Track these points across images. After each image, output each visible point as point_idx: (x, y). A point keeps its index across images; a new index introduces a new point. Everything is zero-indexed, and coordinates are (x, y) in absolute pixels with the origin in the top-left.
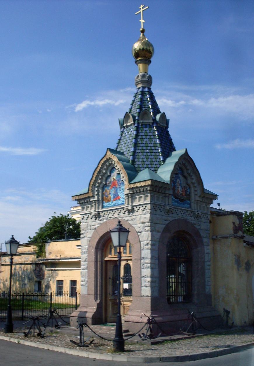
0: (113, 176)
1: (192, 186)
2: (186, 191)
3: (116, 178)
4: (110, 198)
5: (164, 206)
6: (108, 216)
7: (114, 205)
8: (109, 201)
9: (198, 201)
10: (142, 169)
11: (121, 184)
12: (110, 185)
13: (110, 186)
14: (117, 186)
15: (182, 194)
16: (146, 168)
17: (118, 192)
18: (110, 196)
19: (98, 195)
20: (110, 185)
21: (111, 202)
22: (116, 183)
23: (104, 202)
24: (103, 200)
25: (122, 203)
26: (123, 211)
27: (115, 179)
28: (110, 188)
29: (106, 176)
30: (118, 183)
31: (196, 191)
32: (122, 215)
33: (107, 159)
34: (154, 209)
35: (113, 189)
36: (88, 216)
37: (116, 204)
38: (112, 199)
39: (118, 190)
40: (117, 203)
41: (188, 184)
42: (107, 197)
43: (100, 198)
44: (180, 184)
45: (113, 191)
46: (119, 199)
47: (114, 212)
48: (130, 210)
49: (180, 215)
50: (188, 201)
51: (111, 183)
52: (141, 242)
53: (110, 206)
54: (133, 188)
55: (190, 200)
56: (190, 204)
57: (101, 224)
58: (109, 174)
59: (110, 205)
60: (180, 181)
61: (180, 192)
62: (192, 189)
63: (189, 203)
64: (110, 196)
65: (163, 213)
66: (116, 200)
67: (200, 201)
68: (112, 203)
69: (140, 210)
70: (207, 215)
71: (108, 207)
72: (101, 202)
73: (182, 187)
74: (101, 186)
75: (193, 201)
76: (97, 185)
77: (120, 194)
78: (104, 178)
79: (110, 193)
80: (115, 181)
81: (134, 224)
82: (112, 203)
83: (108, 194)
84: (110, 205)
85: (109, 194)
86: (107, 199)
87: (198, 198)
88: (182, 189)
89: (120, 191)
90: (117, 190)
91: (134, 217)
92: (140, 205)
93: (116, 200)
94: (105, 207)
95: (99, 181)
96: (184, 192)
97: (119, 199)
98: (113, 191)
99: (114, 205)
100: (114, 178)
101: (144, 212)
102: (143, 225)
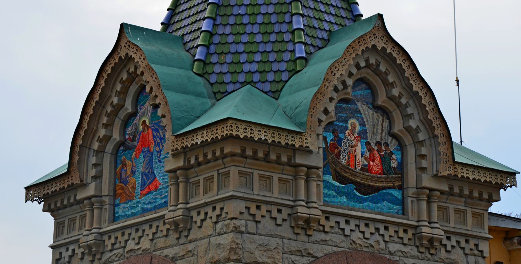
0: (144, 114)
1: (407, 140)
2: (385, 160)
3: (151, 121)
5: (292, 207)
6: (124, 247)
7: (144, 211)
9: (431, 190)
10: (230, 88)
12: (135, 143)
15: (366, 169)
16: (244, 83)
19: (97, 177)
21: (134, 201)
26: (164, 228)
27: (147, 123)
29: (122, 114)
31: (423, 156)
32: (160, 242)
34: (251, 218)
36: (73, 250)
38: (138, 190)
41: (394, 136)
44: (362, 135)
47: (140, 233)
49: (356, 236)
50: (397, 193)
54: (185, 149)
55: (401, 188)
56: (403, 203)
58: (129, 107)
59: (133, 211)
60: (362, 124)
61: (361, 161)
62: (411, 152)
63: (400, 197)
64: (132, 180)
65: (285, 230)
67: (442, 192)
69: (208, 223)
70: (472, 242)
73: (368, 144)
74: (110, 148)
75: (411, 192)
76: (96, 146)
78: (118, 123)
79: (133, 172)
82: (139, 202)
84: (133, 211)
85: (130, 176)
87: (427, 182)
88: (370, 150)
90: (151, 160)
92: (206, 204)
93: (148, 193)
95: (102, 132)
96: (377, 161)
100: (144, 122)
101: (219, 225)
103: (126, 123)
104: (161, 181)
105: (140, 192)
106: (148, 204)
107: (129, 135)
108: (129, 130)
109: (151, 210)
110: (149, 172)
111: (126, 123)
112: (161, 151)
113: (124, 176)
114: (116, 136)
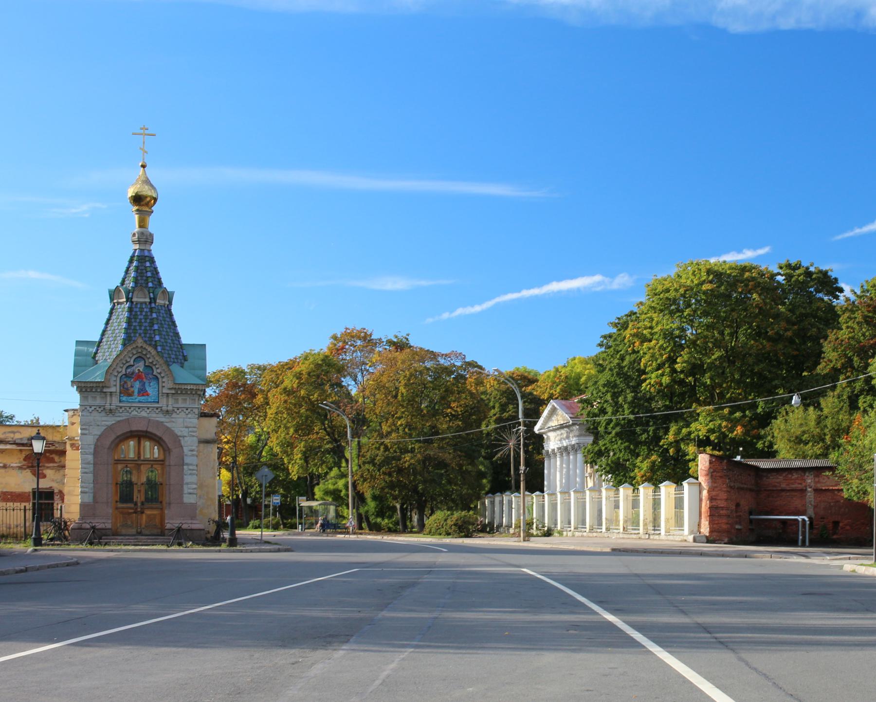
3: (144, 370)
4: (133, 392)
7: (140, 402)
18: (132, 389)
22: (144, 376)
24: (120, 393)
27: (141, 370)
29: (127, 364)
33: (137, 347)
35: (138, 382)
38: (136, 393)
39: (147, 385)
42: (127, 389)
43: (118, 391)
45: (137, 385)
46: (148, 395)
52: (184, 448)
53: (132, 402)
57: (119, 422)
58: (132, 363)
66: (143, 395)
71: (130, 402)
72: (118, 394)
74: (120, 375)
77: (149, 390)
79: (132, 387)
80: (140, 373)
81: (174, 427)
83: (129, 386)
91: (173, 420)
97: (148, 395)
98: (137, 385)
99: (140, 402)
100: (139, 370)
101: (189, 416)
102: (187, 429)
103: (127, 368)
108: (129, 370)
109: (144, 402)
111: (127, 368)
112: (150, 383)
113: (125, 386)
114: (124, 372)
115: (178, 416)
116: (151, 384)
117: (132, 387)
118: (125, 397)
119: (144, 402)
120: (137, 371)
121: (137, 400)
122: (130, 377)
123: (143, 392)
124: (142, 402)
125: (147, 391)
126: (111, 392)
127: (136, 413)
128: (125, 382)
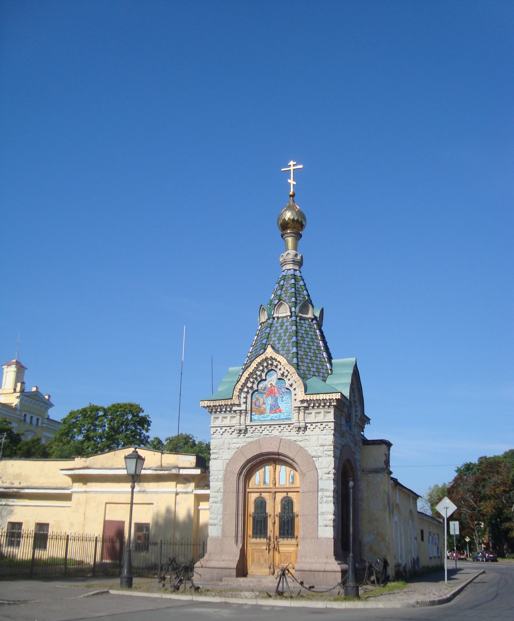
3: (277, 383)
4: (265, 409)
7: (272, 420)
8: (262, 413)
11: (283, 393)
13: (266, 393)
14: (277, 395)
17: (279, 402)
18: (264, 406)
20: (266, 392)
22: (276, 391)
23: (253, 413)
25: (285, 417)
27: (274, 385)
28: (264, 396)
30: (278, 390)
35: (270, 398)
37: (276, 418)
38: (268, 411)
40: (277, 417)
42: (260, 407)
45: (269, 401)
46: (280, 412)
48: (302, 427)
51: (267, 389)
59: (265, 419)
66: (276, 412)
68: (269, 416)
71: (261, 421)
80: (273, 388)
82: (269, 416)
83: (261, 403)
84: (265, 419)
86: (259, 410)
89: (283, 401)
90: (276, 400)
94: (255, 420)
97: (280, 412)
98: (269, 401)
99: (272, 420)
100: (271, 384)
104: (283, 409)
105: (269, 412)
106: (275, 417)
107: (261, 388)
108: (261, 385)
110: (275, 405)
112: (283, 397)
113: (257, 404)
115: (312, 433)
116: (284, 399)
117: (264, 403)
118: (257, 416)
119: (277, 420)
120: (269, 386)
121: (269, 418)
122: (261, 393)
123: (275, 408)
124: (274, 420)
125: (279, 407)
126: (241, 411)
127: (267, 432)
128: (257, 399)
